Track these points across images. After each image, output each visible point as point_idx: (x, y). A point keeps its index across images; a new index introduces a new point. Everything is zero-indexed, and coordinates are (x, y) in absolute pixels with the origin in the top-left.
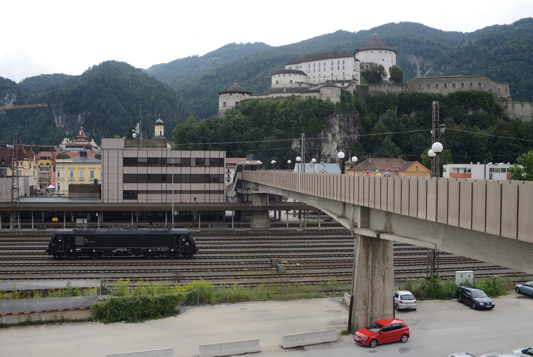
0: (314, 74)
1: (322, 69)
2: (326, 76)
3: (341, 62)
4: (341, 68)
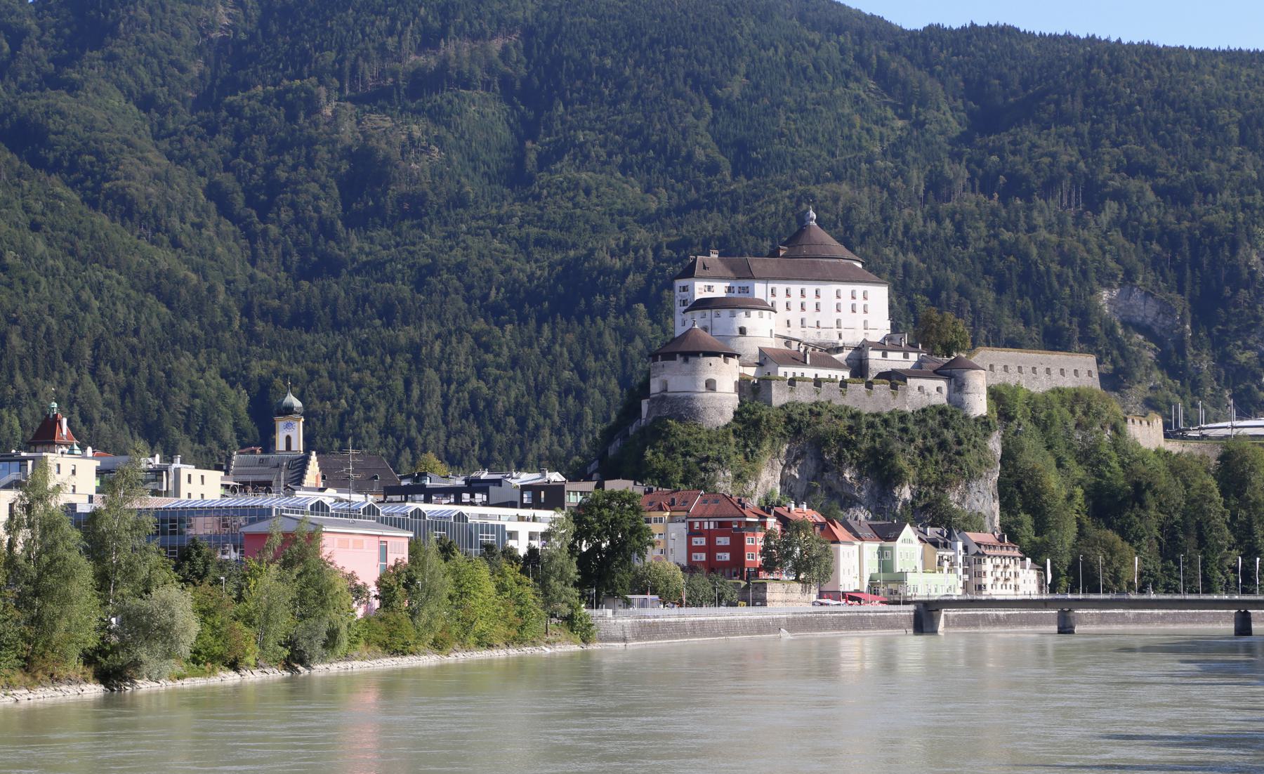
0: (789, 315)
1: (810, 306)
2: (821, 325)
3: (859, 295)
4: (859, 308)
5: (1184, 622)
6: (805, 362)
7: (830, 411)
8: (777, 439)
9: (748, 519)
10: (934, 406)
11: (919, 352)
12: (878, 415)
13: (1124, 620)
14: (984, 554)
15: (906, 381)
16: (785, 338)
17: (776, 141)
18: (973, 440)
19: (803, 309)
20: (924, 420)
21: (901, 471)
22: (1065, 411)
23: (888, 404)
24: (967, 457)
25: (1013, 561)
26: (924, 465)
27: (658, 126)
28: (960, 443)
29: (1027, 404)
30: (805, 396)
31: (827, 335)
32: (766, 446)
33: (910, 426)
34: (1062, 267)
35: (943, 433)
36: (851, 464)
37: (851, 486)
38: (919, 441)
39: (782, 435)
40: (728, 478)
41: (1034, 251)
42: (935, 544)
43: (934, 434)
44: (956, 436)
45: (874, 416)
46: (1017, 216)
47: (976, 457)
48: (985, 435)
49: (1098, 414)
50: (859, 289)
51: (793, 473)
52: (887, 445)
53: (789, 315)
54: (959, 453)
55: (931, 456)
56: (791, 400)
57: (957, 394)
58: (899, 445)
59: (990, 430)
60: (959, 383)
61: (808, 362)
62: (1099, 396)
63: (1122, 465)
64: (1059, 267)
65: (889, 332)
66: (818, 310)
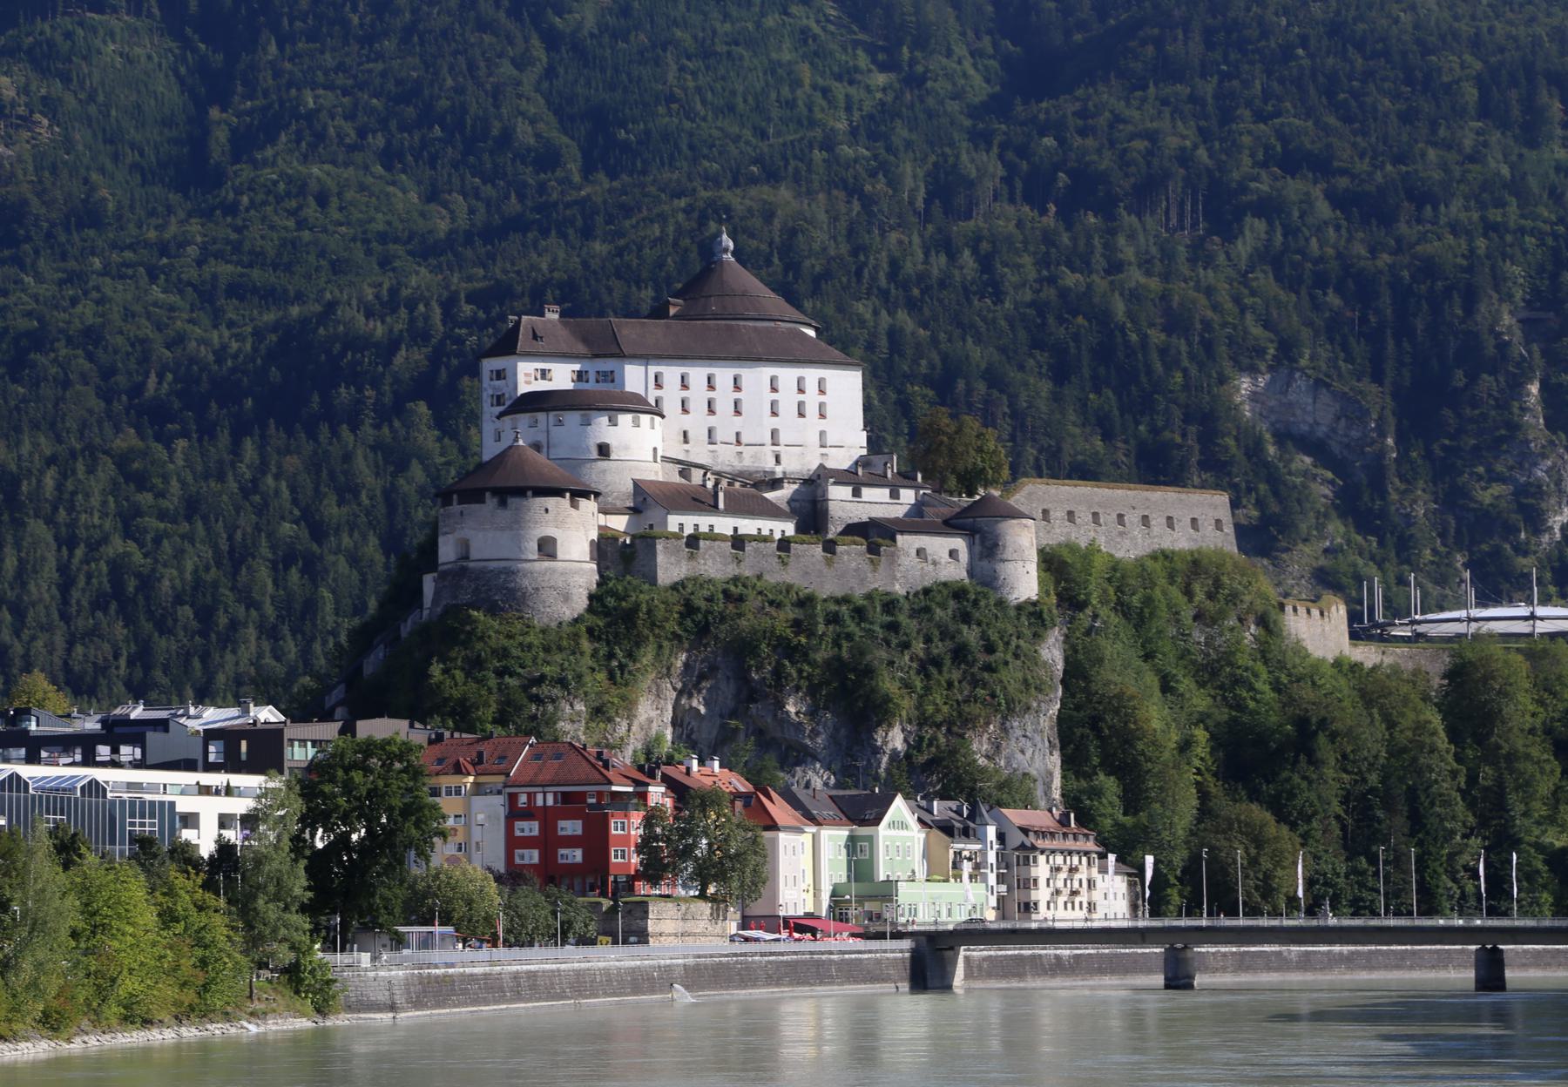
0: (687, 422)
2: (744, 440)
4: (812, 410)
5: (1386, 967)
6: (716, 506)
7: (760, 593)
8: (665, 643)
9: (614, 788)
10: (945, 584)
11: (917, 488)
12: (845, 600)
13: (1281, 964)
14: (1034, 848)
15: (894, 540)
16: (679, 462)
17: (661, 110)
18: (1014, 642)
19: (711, 411)
20: (927, 610)
21: (887, 699)
22: (1175, 593)
23: (862, 581)
24: (1004, 675)
25: (1084, 859)
26: (927, 689)
27: (450, 82)
28: (990, 649)
29: (1109, 580)
30: (715, 567)
31: (755, 457)
32: (647, 656)
33: (903, 618)
34: (1169, 335)
35: (959, 632)
36: (798, 688)
37: (799, 727)
38: (919, 647)
39: (676, 636)
40: (579, 713)
41: (1119, 307)
42: (947, 829)
43: (945, 634)
44: (984, 636)
45: (838, 601)
46: (1089, 244)
47: (1020, 675)
48: (1036, 635)
49: (1233, 598)
50: (812, 375)
51: (695, 703)
52: (862, 653)
53: (687, 422)
54: (989, 668)
55: (940, 672)
56: (691, 574)
57: (985, 563)
58: (883, 654)
59: (1044, 625)
60: (988, 543)
61: (721, 505)
62: (1235, 565)
63: (1277, 687)
64: (1163, 336)
65: (864, 452)
66: (738, 412)
